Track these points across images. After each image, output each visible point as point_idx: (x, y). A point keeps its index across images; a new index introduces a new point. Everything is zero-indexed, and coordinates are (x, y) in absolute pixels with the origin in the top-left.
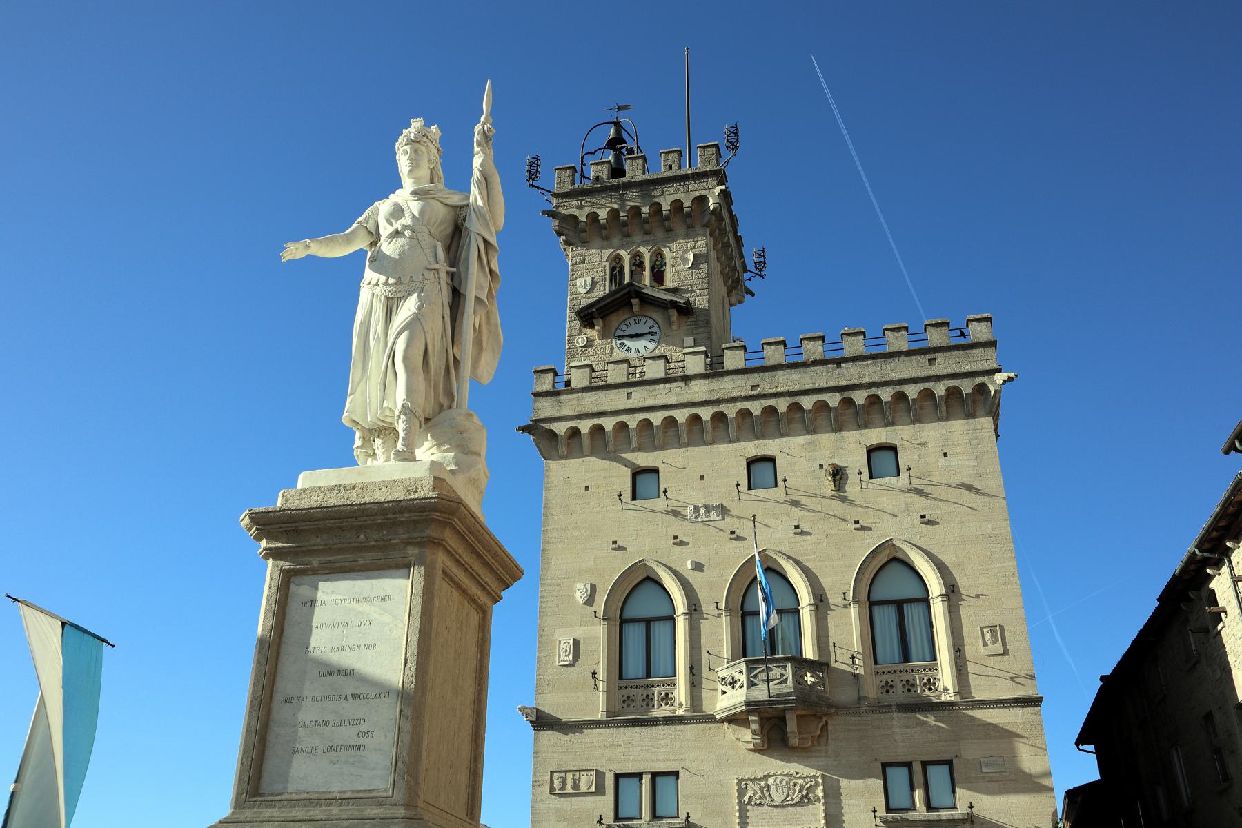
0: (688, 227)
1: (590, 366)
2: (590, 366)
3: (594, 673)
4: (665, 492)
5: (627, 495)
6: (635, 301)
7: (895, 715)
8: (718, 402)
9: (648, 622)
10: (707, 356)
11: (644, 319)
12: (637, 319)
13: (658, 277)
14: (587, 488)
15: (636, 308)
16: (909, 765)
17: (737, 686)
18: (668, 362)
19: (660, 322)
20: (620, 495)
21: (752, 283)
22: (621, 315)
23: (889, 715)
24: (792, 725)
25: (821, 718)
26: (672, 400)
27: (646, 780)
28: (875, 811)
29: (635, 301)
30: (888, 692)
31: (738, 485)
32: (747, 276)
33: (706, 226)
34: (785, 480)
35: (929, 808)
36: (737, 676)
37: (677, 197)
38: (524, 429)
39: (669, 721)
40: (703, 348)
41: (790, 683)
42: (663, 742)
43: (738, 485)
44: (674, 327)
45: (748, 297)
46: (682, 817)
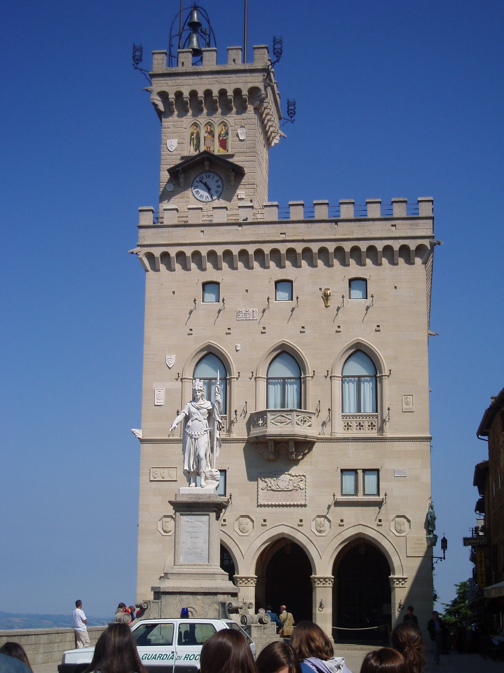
6: (207, 163)
13: (223, 144)
14: (174, 292)
29: (207, 163)
46: (228, 497)
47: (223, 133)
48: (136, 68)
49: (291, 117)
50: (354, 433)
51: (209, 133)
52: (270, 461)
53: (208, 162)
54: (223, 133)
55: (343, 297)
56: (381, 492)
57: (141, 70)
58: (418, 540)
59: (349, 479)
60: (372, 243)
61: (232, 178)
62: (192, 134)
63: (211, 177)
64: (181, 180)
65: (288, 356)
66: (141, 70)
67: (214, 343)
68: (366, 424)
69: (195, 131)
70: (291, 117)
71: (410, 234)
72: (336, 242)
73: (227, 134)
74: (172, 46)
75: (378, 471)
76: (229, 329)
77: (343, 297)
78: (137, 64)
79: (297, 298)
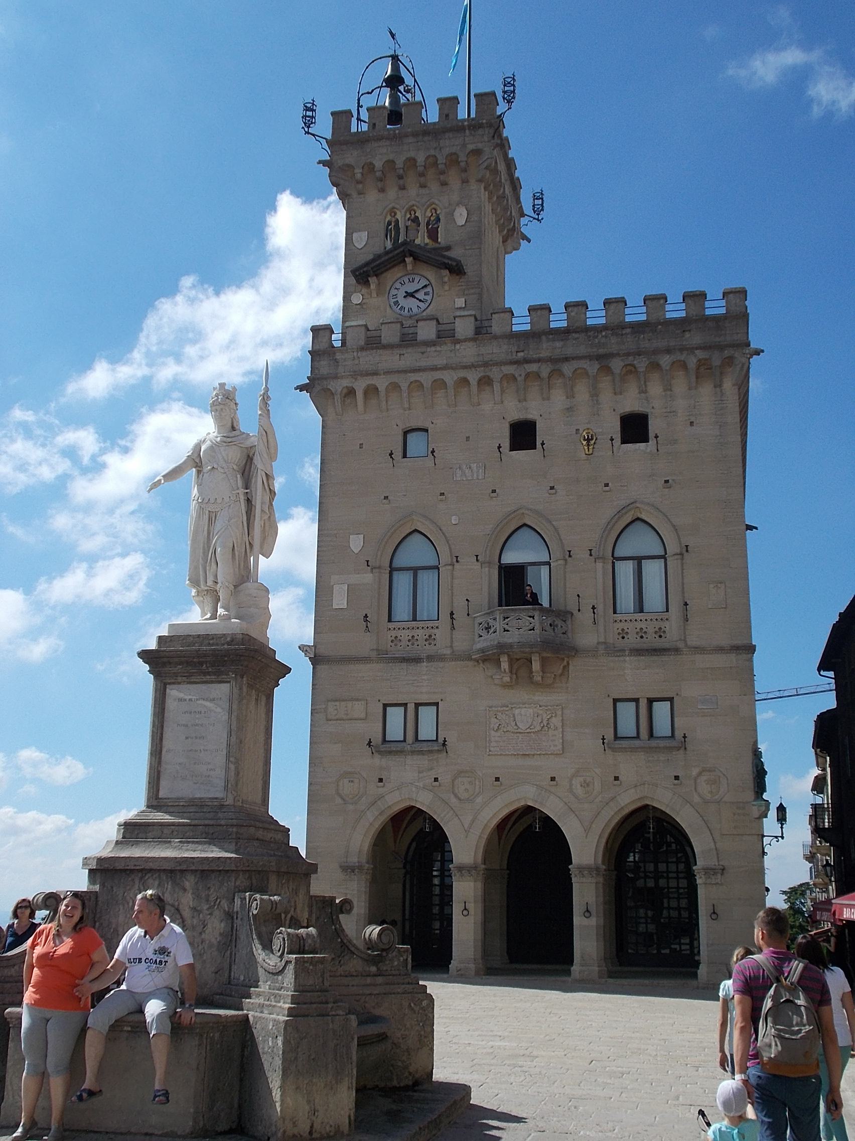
0: (463, 182)
1: (366, 326)
2: (366, 326)
3: (366, 616)
4: (433, 452)
5: (398, 454)
6: (409, 260)
8: (486, 365)
9: (415, 570)
10: (476, 320)
11: (417, 279)
12: (411, 277)
13: (433, 234)
15: (409, 267)
17: (492, 631)
19: (433, 281)
20: (391, 454)
21: (527, 226)
22: (396, 273)
24: (536, 666)
25: (563, 659)
26: (440, 361)
27: (411, 707)
29: (409, 260)
30: (623, 638)
31: (499, 447)
32: (524, 221)
33: (480, 181)
34: (543, 444)
36: (491, 622)
37: (453, 150)
38: (301, 388)
39: (430, 658)
40: (473, 313)
41: (537, 631)
42: (425, 677)
43: (499, 447)
44: (447, 288)
45: (524, 243)
47: (432, 219)
48: (308, 133)
49: (538, 214)
51: (413, 221)
52: (505, 686)
53: (411, 258)
54: (432, 219)
55: (612, 440)
57: (314, 135)
61: (446, 279)
62: (389, 223)
63: (416, 280)
64: (373, 286)
65: (533, 533)
66: (314, 135)
69: (393, 220)
70: (538, 214)
73: (438, 220)
74: (362, 107)
76: (442, 494)
77: (612, 440)
78: (309, 127)
79: (543, 444)
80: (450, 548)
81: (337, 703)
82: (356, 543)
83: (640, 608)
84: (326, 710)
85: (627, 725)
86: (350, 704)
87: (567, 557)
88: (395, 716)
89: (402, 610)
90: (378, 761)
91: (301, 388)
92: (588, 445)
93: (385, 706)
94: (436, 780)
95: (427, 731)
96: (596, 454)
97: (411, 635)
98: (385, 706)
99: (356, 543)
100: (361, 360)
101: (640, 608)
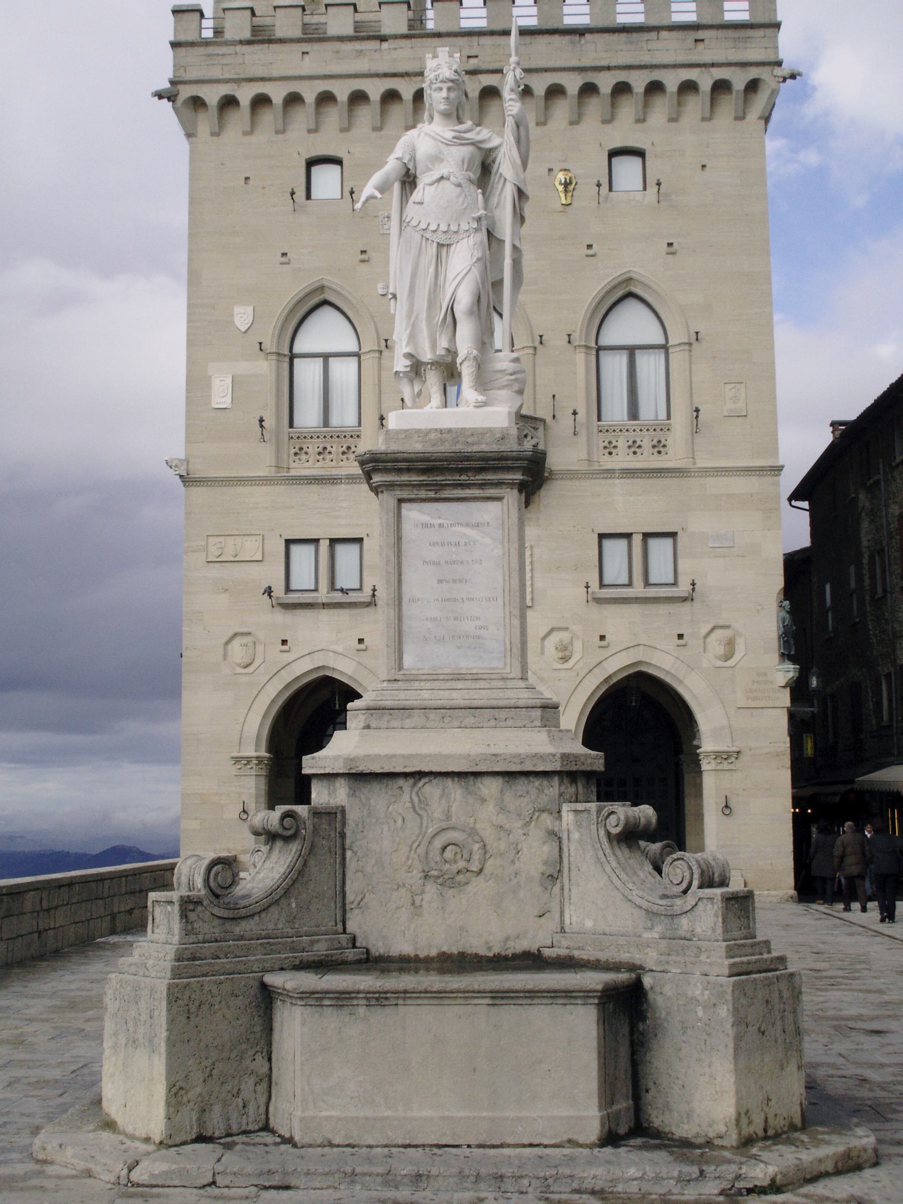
3: (261, 420)
7: (617, 481)
16: (628, 536)
18: (356, 10)
20: (292, 194)
23: (610, 481)
28: (587, 587)
30: (610, 453)
35: (647, 584)
38: (160, 95)
42: (344, 504)
46: (368, 590)
50: (622, 460)
55: (599, 185)
56: (681, 579)
58: (759, 674)
59: (616, 550)
60: (656, 75)
67: (330, 280)
68: (647, 444)
71: (734, 57)
72: (583, 74)
75: (673, 535)
76: (363, 252)
80: (376, 327)
81: (222, 539)
82: (242, 317)
83: (634, 413)
84: (206, 549)
85: (615, 570)
86: (239, 540)
87: (537, 343)
88: (302, 556)
89: (308, 415)
90: (281, 617)
91: (160, 95)
92: (566, 191)
93: (288, 542)
94: (361, 641)
95: (347, 577)
96: (575, 204)
97: (321, 446)
98: (288, 542)
99: (242, 317)
100: (247, 57)
101: (634, 413)
